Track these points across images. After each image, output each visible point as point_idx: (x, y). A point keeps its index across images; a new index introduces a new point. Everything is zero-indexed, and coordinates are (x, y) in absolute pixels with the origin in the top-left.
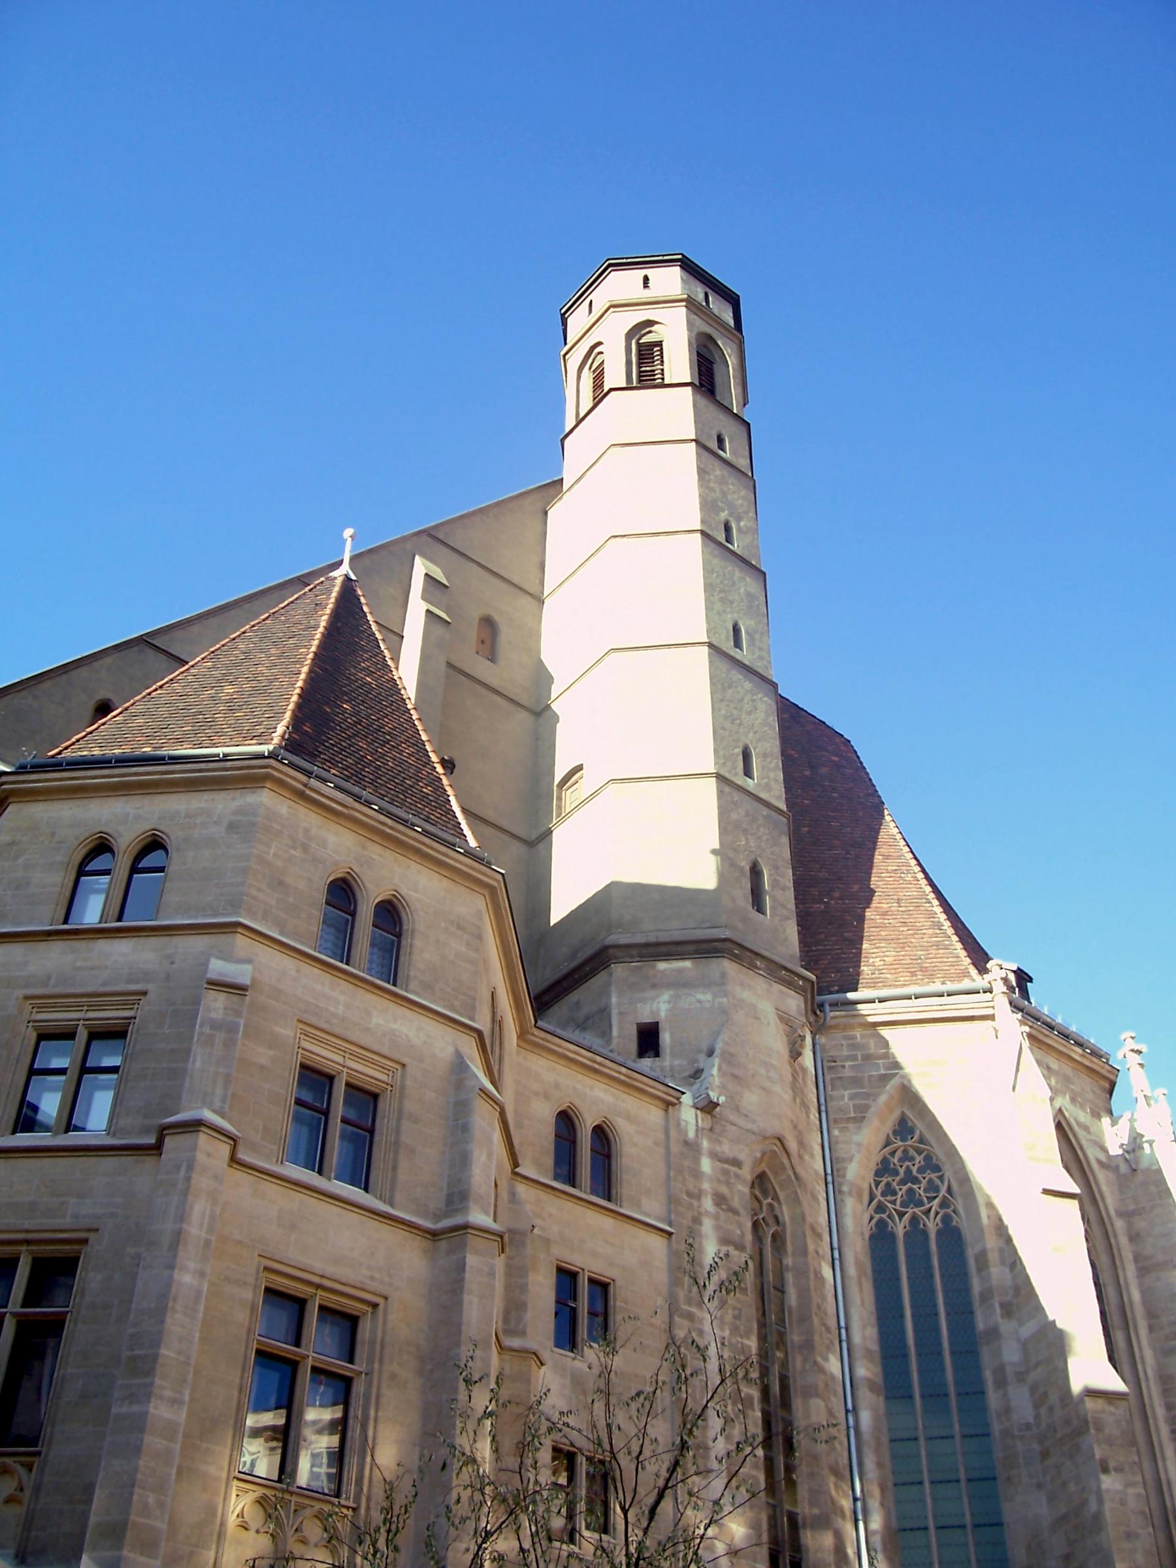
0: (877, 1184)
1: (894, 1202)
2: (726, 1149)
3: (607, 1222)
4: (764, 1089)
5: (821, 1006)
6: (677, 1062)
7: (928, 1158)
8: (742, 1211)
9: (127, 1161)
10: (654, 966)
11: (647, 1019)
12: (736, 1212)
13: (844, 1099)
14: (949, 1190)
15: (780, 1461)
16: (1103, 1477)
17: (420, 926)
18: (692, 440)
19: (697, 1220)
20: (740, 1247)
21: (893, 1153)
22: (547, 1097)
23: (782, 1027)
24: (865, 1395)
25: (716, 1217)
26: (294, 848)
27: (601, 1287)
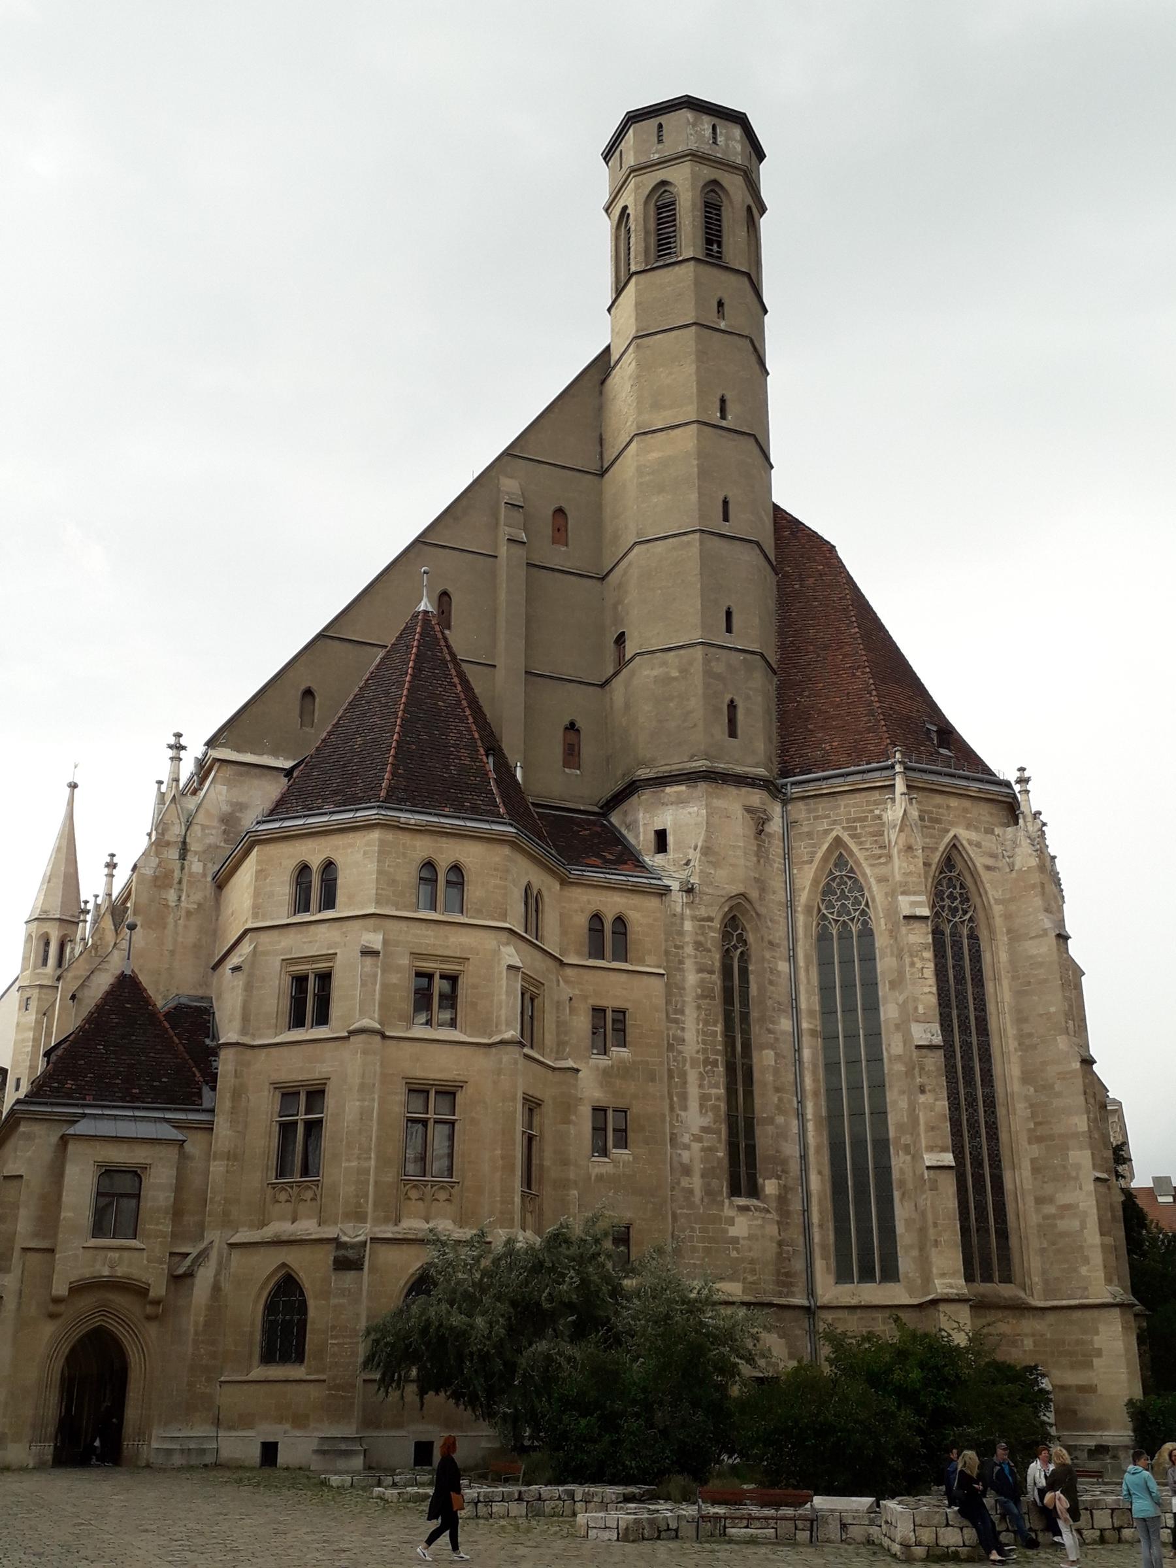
1: (832, 913)
2: (703, 912)
3: (624, 977)
4: (731, 865)
7: (856, 881)
8: (713, 949)
9: (338, 1043)
12: (710, 951)
13: (801, 848)
14: (867, 905)
16: (921, 1096)
18: (695, 324)
19: (681, 962)
20: (711, 972)
21: (834, 879)
23: (747, 816)
24: (806, 1039)
27: (621, 1013)
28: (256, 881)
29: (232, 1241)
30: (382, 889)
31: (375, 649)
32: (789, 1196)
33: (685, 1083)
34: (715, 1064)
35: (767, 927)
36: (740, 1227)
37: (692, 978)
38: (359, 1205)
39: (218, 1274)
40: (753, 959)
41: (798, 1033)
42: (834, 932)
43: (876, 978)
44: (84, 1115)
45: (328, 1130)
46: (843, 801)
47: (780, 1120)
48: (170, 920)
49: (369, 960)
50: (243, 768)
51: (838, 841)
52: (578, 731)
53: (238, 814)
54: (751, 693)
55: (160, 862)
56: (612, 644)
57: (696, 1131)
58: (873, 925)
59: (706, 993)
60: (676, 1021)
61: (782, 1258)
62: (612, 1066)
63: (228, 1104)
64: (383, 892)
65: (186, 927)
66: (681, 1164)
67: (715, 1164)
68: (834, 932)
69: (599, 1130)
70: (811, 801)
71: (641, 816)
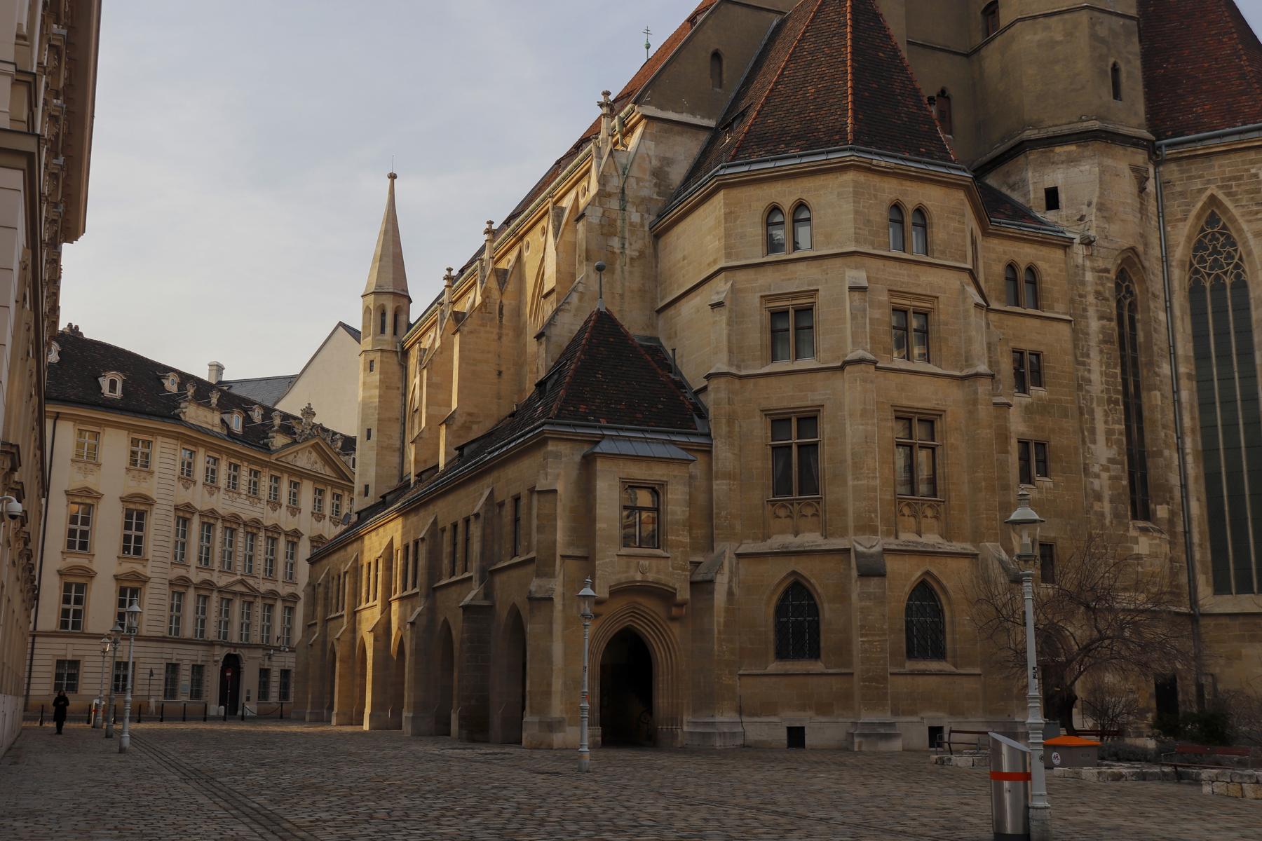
0: (1195, 256)
1: (1205, 268)
2: (1101, 264)
3: (1037, 322)
5: (1160, 147)
6: (1069, 212)
7: (1229, 237)
8: (1111, 299)
9: (829, 373)
10: (1053, 151)
11: (1050, 184)
13: (1174, 207)
14: (1241, 259)
15: (1135, 427)
17: (935, 220)
19: (1085, 310)
20: (1110, 320)
21: (1205, 237)
22: (1000, 262)
24: (1184, 383)
25: (1097, 306)
26: (871, 199)
28: (726, 223)
29: (739, 551)
30: (860, 229)
31: (771, 15)
32: (1175, 520)
33: (1093, 419)
34: (1116, 402)
35: (1151, 280)
36: (1143, 546)
37: (1094, 325)
38: (871, 519)
39: (730, 581)
40: (1139, 309)
41: (1176, 377)
42: (1208, 285)
43: (1251, 326)
44: (603, 436)
45: (825, 453)
46: (1217, 162)
47: (1166, 453)
48: (618, 266)
49: (857, 295)
50: (666, 126)
51: (1213, 199)
52: (948, 98)
53: (666, 169)
54: (1131, 57)
55: (604, 212)
56: (979, 13)
57: (1104, 462)
58: (1248, 277)
59: (1107, 339)
60: (1083, 364)
61: (1174, 574)
62: (1032, 404)
63: (724, 429)
64: (861, 232)
65: (631, 273)
66: (1094, 491)
67: (1120, 491)
68: (1208, 285)
69: (1024, 458)
70: (1184, 163)
71: (1030, 175)
